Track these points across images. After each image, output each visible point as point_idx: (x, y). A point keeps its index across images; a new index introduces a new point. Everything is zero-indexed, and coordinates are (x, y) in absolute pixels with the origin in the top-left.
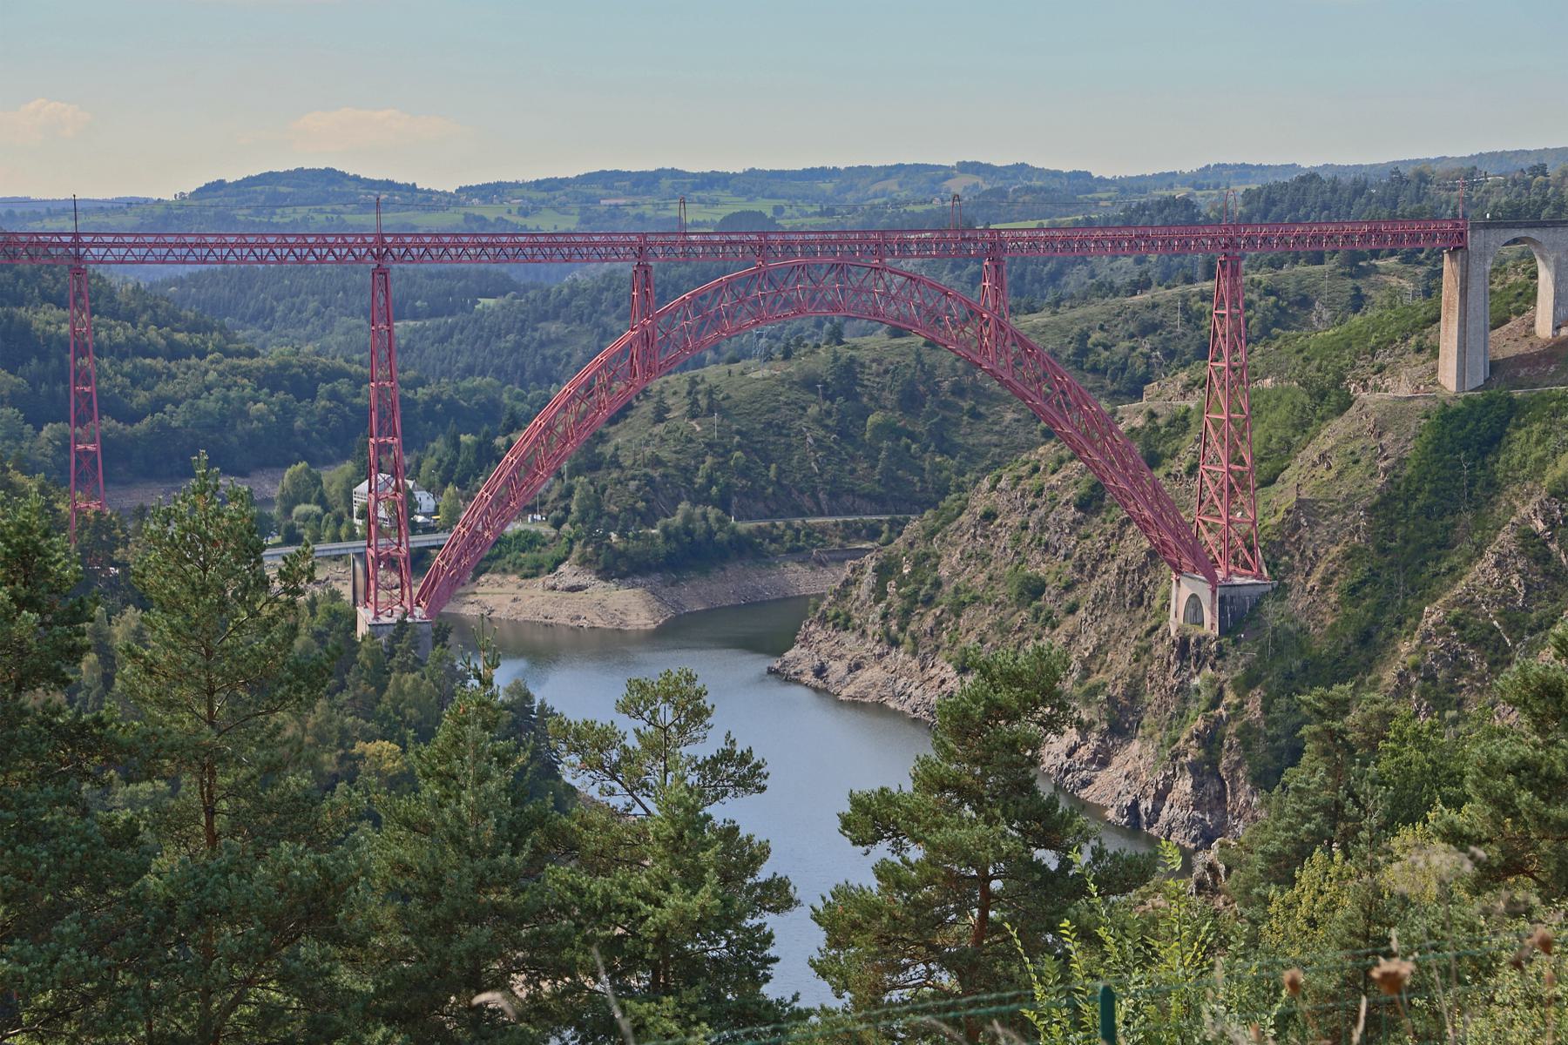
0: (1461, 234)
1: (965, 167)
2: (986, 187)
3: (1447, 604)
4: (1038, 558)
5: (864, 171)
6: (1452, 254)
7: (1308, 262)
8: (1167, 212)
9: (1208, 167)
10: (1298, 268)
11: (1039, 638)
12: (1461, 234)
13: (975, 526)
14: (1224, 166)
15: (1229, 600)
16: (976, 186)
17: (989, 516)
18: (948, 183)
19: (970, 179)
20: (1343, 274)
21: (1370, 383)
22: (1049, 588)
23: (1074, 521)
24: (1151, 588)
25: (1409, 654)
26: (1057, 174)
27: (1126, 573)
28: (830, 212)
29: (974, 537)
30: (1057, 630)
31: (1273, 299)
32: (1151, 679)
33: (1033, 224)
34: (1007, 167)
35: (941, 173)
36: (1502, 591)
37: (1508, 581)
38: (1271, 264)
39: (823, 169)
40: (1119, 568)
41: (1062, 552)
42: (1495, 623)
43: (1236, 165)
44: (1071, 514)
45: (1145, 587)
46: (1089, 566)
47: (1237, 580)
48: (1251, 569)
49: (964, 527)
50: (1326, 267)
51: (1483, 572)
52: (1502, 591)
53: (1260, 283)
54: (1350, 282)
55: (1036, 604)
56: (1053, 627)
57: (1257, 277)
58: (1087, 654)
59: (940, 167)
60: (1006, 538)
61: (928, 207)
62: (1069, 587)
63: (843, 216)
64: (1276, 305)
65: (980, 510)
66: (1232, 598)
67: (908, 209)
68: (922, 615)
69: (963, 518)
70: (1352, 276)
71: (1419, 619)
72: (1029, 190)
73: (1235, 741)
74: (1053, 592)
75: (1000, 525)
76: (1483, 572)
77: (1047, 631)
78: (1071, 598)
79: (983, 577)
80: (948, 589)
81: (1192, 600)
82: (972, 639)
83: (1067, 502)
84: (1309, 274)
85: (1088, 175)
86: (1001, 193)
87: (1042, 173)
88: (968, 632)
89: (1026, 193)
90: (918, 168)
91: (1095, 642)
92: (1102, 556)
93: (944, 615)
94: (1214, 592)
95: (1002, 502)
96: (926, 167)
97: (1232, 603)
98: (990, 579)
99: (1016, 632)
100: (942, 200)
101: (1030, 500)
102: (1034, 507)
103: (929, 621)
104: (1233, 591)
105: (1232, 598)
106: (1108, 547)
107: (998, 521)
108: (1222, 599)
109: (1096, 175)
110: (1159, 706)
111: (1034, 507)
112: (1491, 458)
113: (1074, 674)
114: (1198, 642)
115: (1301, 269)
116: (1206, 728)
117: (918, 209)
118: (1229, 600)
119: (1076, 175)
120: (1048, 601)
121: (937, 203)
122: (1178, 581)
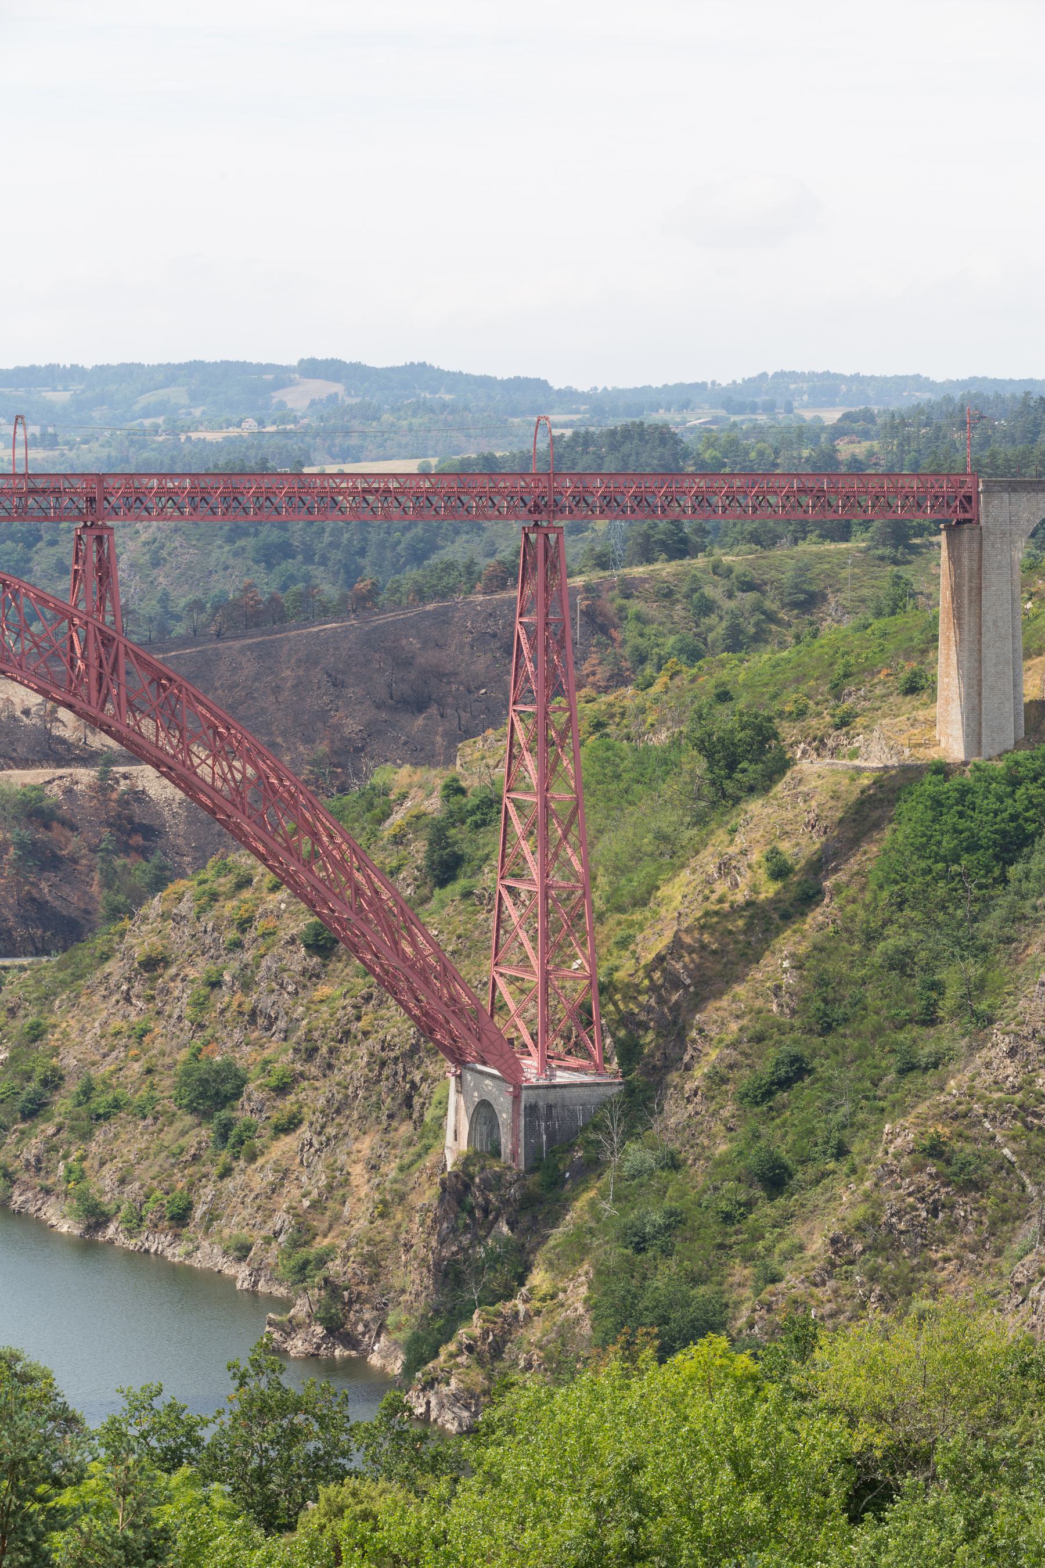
0: (969, 499)
1: (312, 368)
2: (349, 401)
3: (923, 1120)
4: (237, 1035)
5: (129, 372)
6: (954, 529)
7: (824, 537)
8: (626, 448)
9: (763, 376)
10: (803, 546)
11: (226, 1173)
12: (969, 499)
13: (129, 980)
14: (793, 376)
15: (543, 1111)
16: (333, 398)
17: (152, 964)
18: (277, 396)
19: (320, 388)
20: (882, 558)
21: (830, 743)
22: (251, 1086)
23: (303, 973)
24: (424, 1088)
25: (852, 1205)
26: (485, 382)
27: (383, 1064)
28: (50, 441)
29: (128, 999)
30: (260, 1161)
31: (751, 596)
32: (408, 1247)
33: (411, 466)
34: (393, 370)
35: (269, 377)
36: (1019, 1097)
37: (1031, 1082)
38: (755, 539)
39: (51, 369)
40: (372, 1055)
41: (281, 1024)
42: (1006, 1151)
43: (813, 375)
44: (299, 958)
45: (414, 1086)
46: (324, 1050)
47: (562, 1077)
48: (589, 1056)
49: (112, 982)
50: (857, 544)
51: (988, 1065)
52: (1019, 1097)
53: (730, 570)
54: (891, 569)
55: (224, 1114)
56: (252, 1158)
57: (728, 559)
58: (306, 1203)
59: (270, 368)
60: (182, 1004)
61: (233, 432)
62: (282, 1089)
63: (71, 444)
64: (758, 608)
65: (139, 953)
66: (550, 1107)
67: (194, 436)
68: (23, 1133)
69: (109, 967)
70: (896, 562)
71: (876, 1142)
72: (420, 407)
73: (537, 1355)
74: (257, 1096)
75: (173, 979)
76: (988, 1065)
77: (242, 1163)
78: (288, 1104)
79: (137, 1067)
80: (73, 1086)
81: (483, 1111)
82: (108, 1178)
83: (292, 941)
84: (820, 557)
85: (542, 385)
86: (370, 414)
87: (455, 380)
88: (102, 1164)
89: (415, 414)
90: (228, 370)
91: (323, 1181)
92: (347, 1033)
93: (64, 1135)
94: (516, 1098)
95: (179, 937)
96: (243, 367)
97: (549, 1117)
98: (149, 1071)
99: (187, 1164)
100: (261, 423)
101: (232, 934)
102: (237, 945)
103: (33, 1147)
104: (552, 1096)
105: (550, 1107)
106: (359, 1018)
107: (173, 971)
108: (532, 1110)
109: (557, 383)
110: (417, 1295)
111: (237, 945)
112: (1014, 871)
113: (282, 1238)
114: (487, 1186)
115: (810, 547)
116: (486, 1333)
117: (214, 437)
118: (543, 1111)
119: (519, 384)
120: (242, 1113)
121: (250, 425)
122: (459, 1077)
